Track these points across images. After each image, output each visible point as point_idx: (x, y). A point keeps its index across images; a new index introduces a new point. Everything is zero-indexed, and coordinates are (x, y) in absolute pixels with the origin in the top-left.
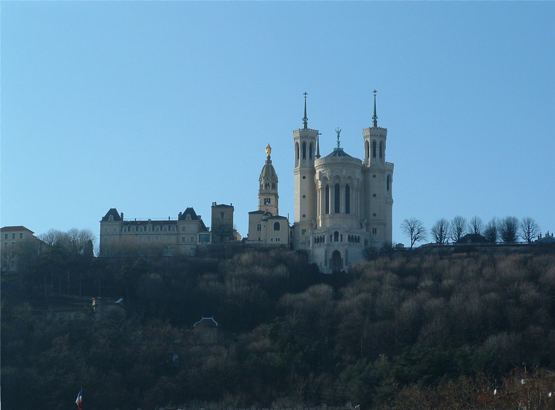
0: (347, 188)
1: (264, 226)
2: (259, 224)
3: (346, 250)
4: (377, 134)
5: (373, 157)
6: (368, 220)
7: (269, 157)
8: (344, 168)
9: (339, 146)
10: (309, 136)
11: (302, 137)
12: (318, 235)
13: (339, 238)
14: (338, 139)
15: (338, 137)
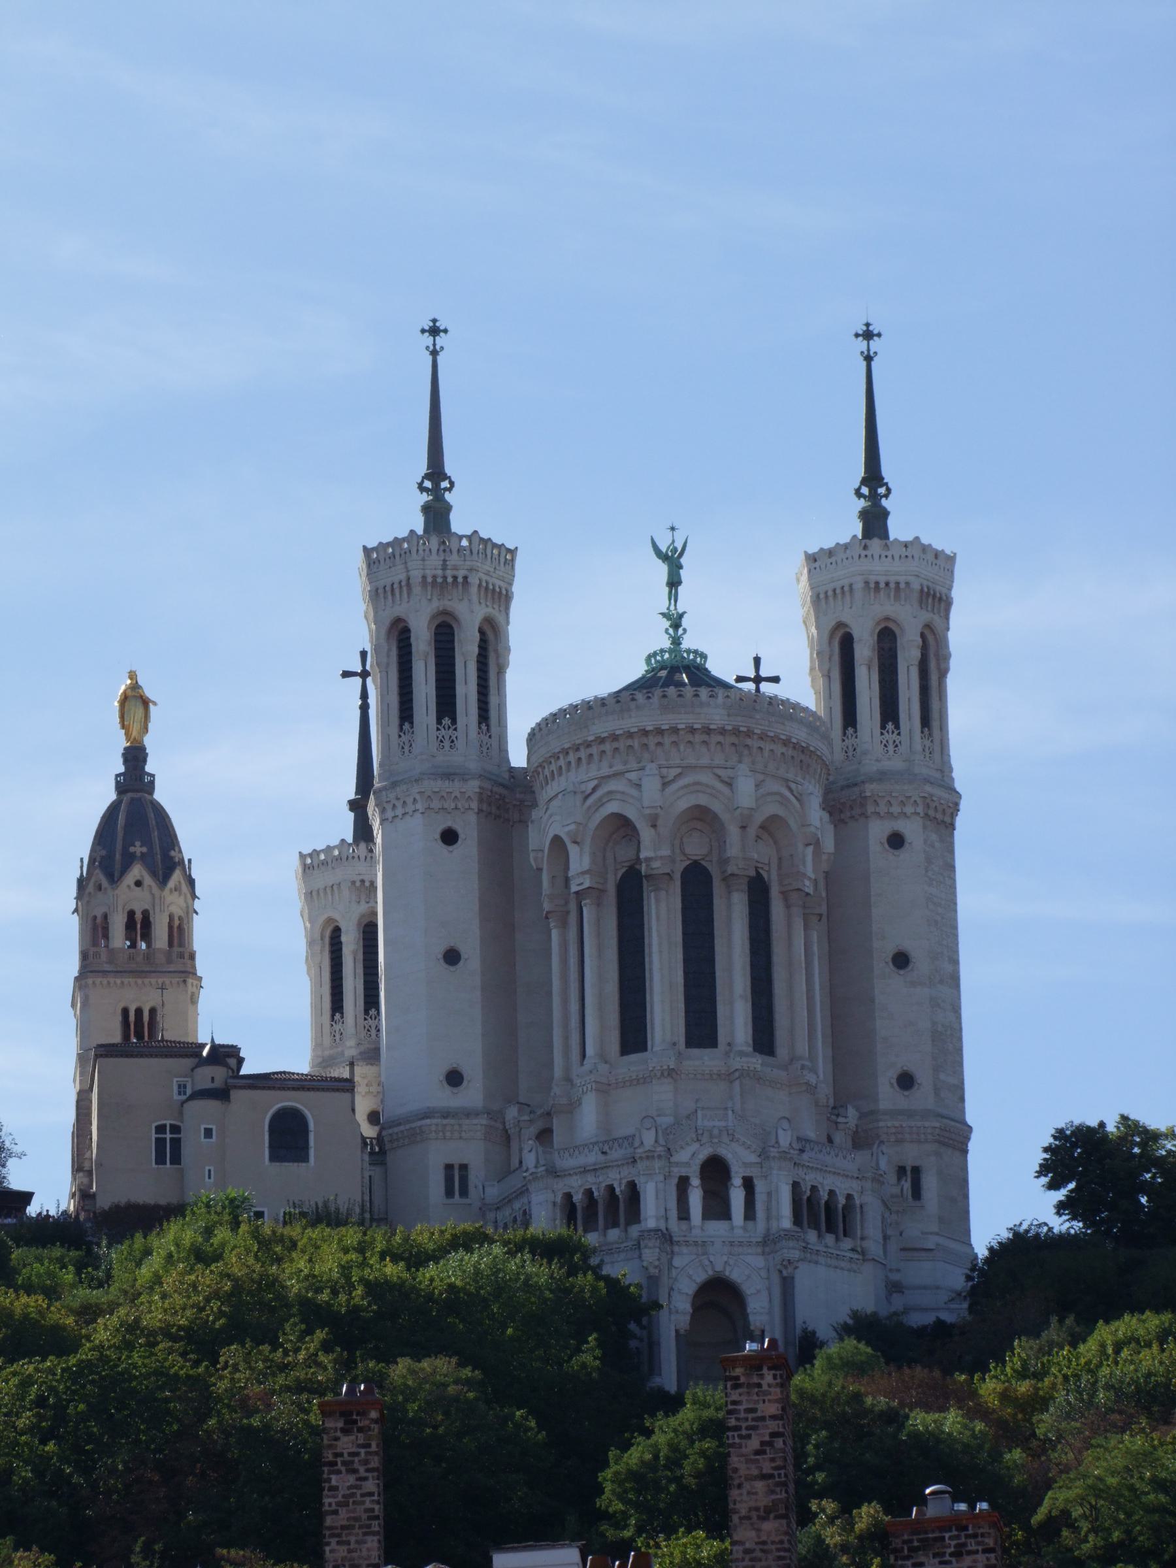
0: (758, 891)
1: (208, 1133)
2: (168, 1123)
3: (785, 1273)
4: (907, 584)
5: (883, 727)
6: (862, 1116)
7: (135, 756)
8: (740, 762)
9: (676, 641)
10: (474, 580)
11: (434, 582)
12: (590, 1181)
13: (737, 1197)
14: (673, 595)
15: (674, 583)
